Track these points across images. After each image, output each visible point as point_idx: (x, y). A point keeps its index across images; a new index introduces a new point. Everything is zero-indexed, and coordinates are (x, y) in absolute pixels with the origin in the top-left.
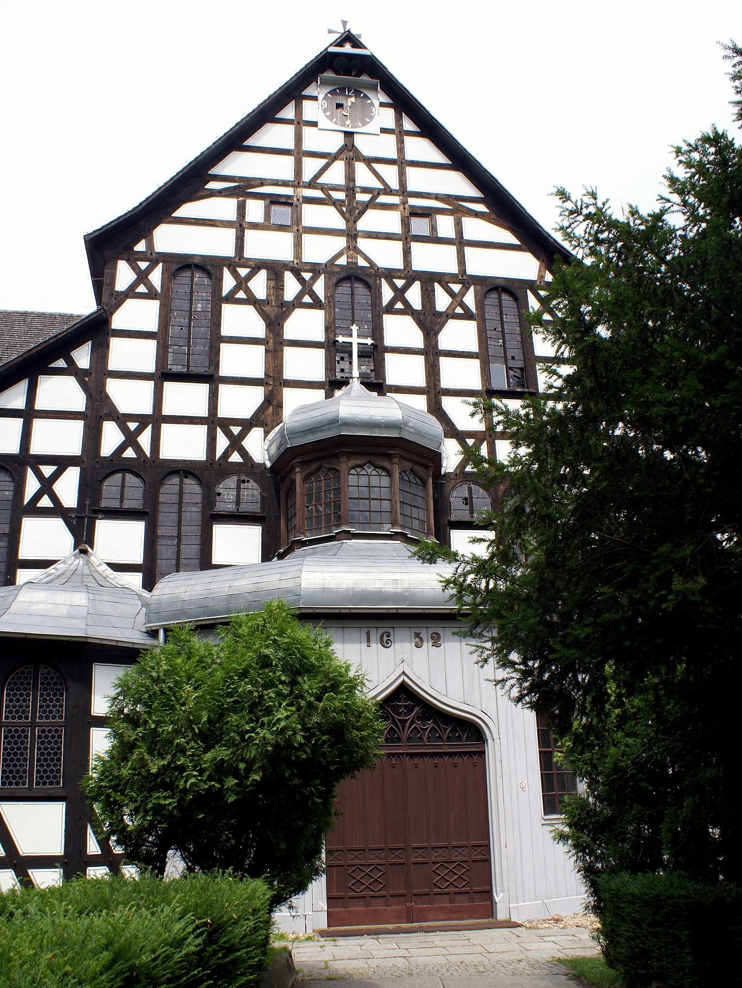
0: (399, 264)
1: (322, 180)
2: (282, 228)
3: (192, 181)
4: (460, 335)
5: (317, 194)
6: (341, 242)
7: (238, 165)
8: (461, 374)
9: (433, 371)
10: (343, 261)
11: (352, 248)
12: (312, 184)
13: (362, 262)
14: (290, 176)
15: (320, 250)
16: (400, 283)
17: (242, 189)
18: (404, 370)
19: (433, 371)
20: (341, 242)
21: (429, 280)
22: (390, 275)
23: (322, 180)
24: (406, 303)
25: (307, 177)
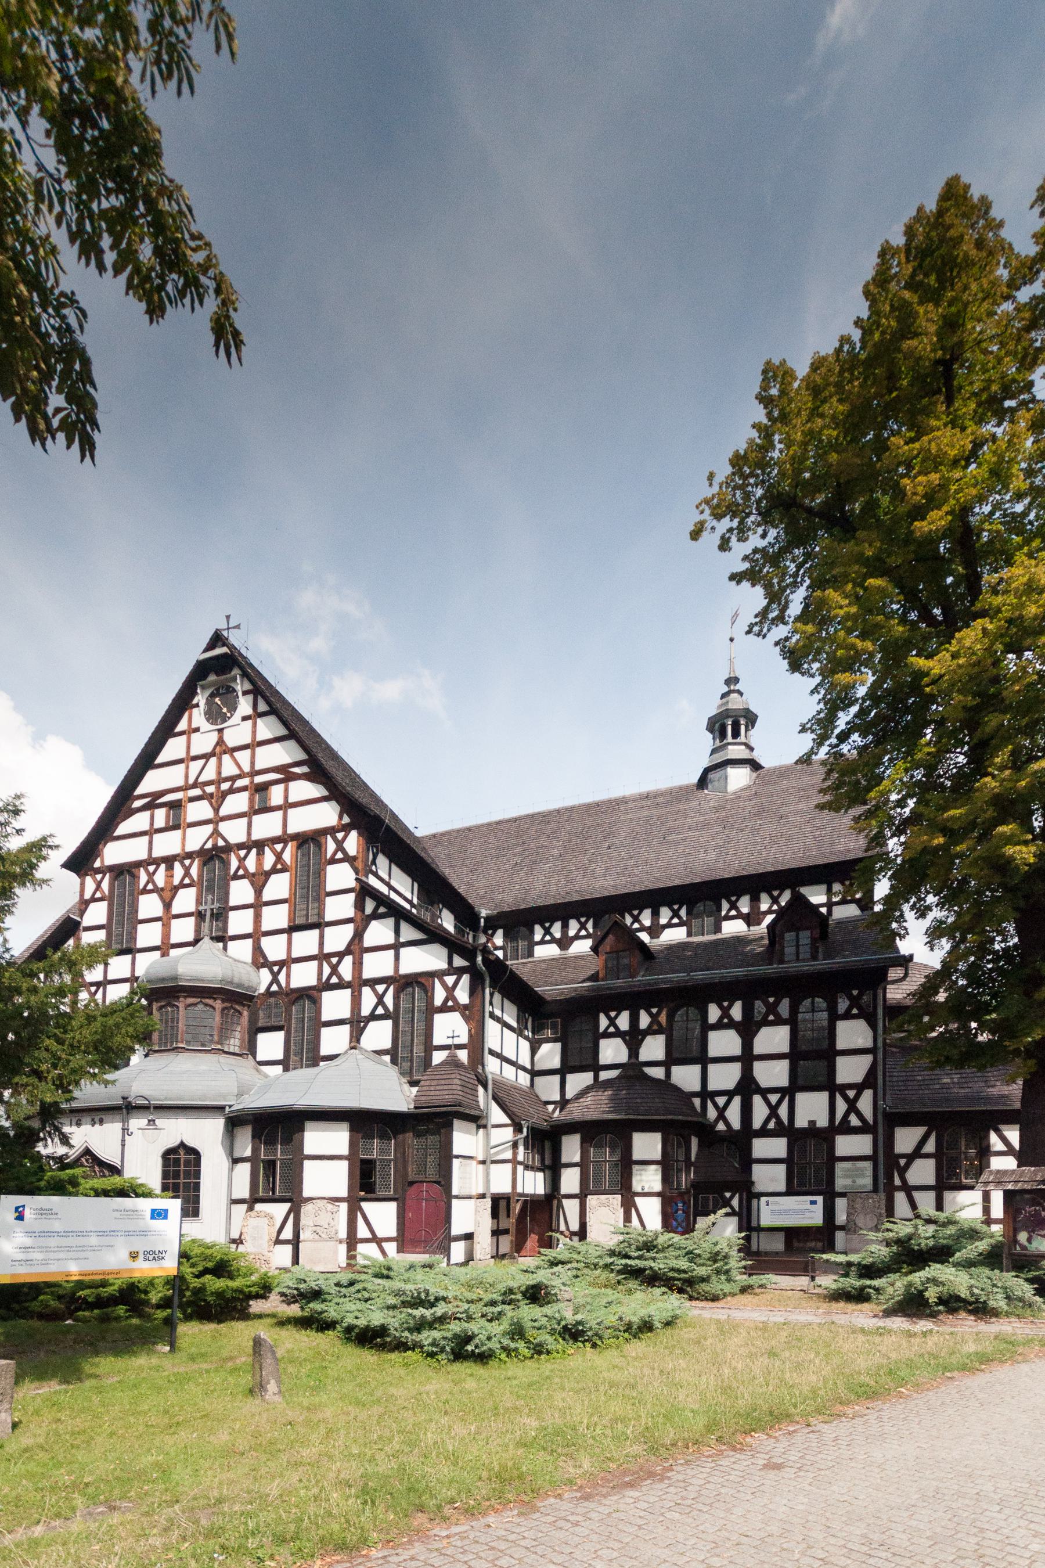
0: (242, 838)
1: (200, 780)
2: (176, 827)
3: (121, 805)
4: (279, 886)
5: (197, 792)
6: (209, 829)
7: (152, 782)
8: (276, 917)
9: (257, 919)
10: (209, 845)
11: (216, 833)
12: (195, 785)
13: (221, 843)
14: (181, 783)
15: (197, 839)
16: (242, 853)
17: (153, 802)
18: (239, 922)
19: (257, 919)
20: (209, 829)
21: (260, 845)
22: (240, 846)
23: (200, 780)
24: (246, 869)
25: (191, 781)
